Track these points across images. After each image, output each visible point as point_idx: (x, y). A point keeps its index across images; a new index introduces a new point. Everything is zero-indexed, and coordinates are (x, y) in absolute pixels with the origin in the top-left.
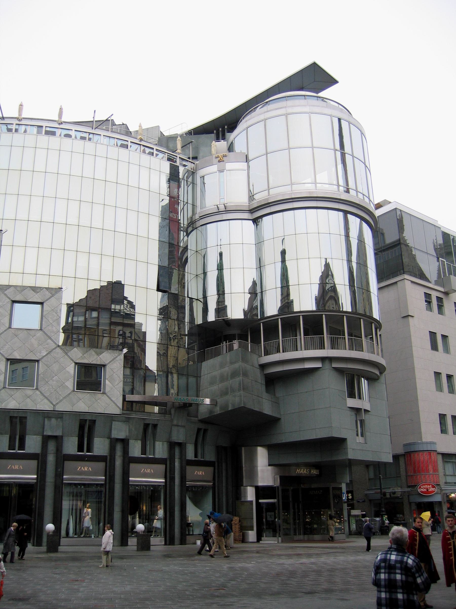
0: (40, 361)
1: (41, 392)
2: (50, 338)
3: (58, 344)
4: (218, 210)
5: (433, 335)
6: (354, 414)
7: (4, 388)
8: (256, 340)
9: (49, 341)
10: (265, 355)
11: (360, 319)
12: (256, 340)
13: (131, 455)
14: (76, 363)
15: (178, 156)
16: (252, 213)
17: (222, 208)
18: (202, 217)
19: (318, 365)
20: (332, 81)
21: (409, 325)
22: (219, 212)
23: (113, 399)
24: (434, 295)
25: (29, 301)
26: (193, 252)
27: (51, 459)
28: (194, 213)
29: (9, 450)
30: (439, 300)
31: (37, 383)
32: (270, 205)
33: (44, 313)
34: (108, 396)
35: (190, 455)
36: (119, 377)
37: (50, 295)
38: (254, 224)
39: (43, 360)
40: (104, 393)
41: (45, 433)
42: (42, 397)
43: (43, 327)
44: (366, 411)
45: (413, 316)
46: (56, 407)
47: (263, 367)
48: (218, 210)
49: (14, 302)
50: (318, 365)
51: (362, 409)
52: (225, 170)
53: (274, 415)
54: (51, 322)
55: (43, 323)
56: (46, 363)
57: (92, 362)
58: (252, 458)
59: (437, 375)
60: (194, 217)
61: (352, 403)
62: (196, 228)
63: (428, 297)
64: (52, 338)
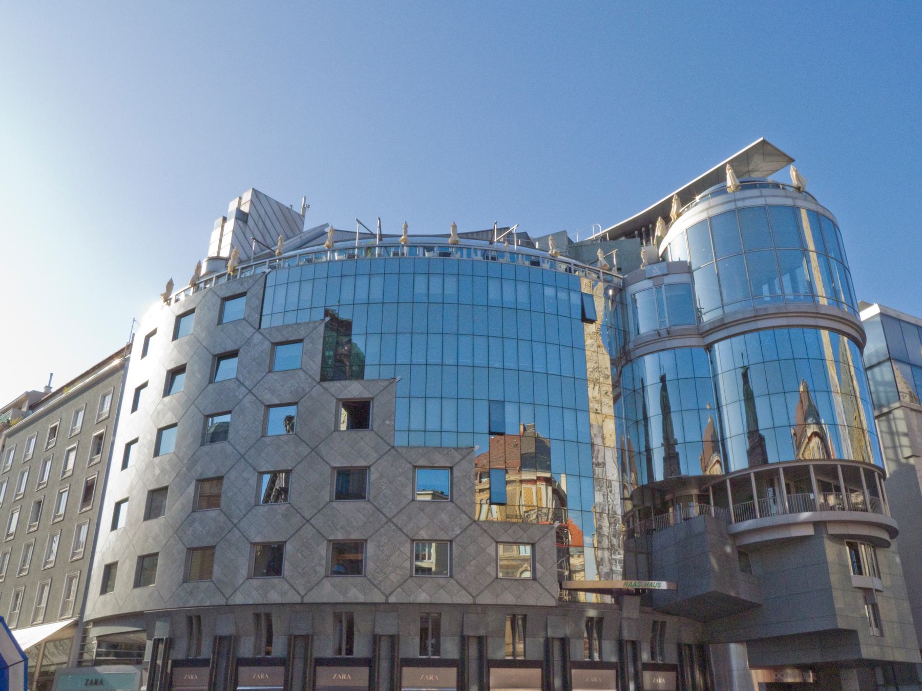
0: (454, 542)
1: (456, 581)
2: (463, 512)
4: (660, 336)
6: (862, 597)
7: (411, 576)
8: (721, 502)
9: (463, 516)
10: (737, 521)
11: (858, 468)
12: (721, 502)
15: (601, 271)
16: (703, 337)
18: (637, 347)
23: (547, 587)
25: (435, 465)
26: (629, 392)
28: (626, 342)
29: (421, 655)
31: (451, 569)
32: (727, 326)
33: (455, 480)
34: (540, 584)
35: (645, 657)
39: (457, 540)
41: (465, 633)
43: (455, 497)
44: (877, 590)
46: (477, 599)
47: (735, 536)
49: (415, 467)
50: (810, 531)
53: (754, 601)
54: (464, 491)
55: (454, 492)
56: (460, 544)
58: (726, 659)
60: (627, 347)
62: (631, 360)
64: (467, 512)
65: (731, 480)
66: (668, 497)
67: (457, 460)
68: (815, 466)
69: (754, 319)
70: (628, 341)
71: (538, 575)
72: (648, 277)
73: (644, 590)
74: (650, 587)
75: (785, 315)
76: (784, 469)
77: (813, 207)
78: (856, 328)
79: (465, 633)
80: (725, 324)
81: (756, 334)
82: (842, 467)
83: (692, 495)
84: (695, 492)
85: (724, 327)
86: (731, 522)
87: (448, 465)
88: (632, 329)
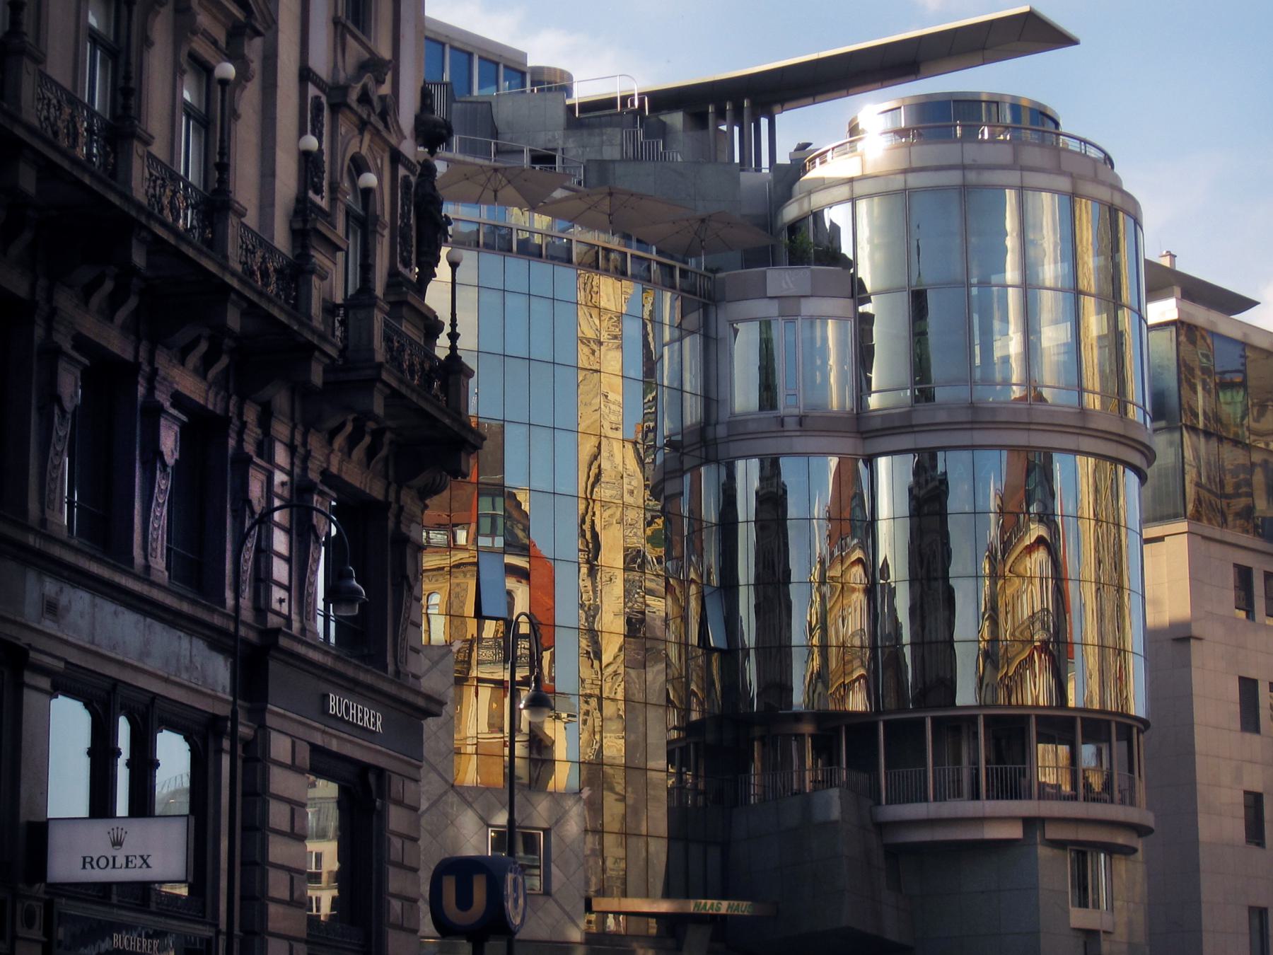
3: (451, 781)
8: (863, 759)
11: (1109, 722)
12: (863, 759)
16: (866, 438)
17: (791, 424)
20: (1059, 39)
21: (1187, 665)
22: (784, 431)
23: (568, 908)
32: (916, 429)
34: (556, 902)
38: (867, 467)
45: (1200, 639)
47: (882, 827)
48: (783, 426)
50: (1015, 832)
52: (799, 318)
56: (429, 828)
57: (522, 821)
60: (710, 429)
62: (718, 462)
63: (1244, 576)
65: (886, 723)
66: (757, 731)
68: (1037, 717)
69: (969, 426)
70: (713, 421)
71: (555, 886)
72: (768, 295)
73: (724, 917)
74: (736, 913)
75: (1027, 427)
76: (985, 716)
77: (1104, 194)
78: (1142, 448)
80: (912, 426)
81: (966, 455)
82: (1083, 719)
83: (803, 735)
84: (807, 728)
85: (910, 430)
86: (879, 803)
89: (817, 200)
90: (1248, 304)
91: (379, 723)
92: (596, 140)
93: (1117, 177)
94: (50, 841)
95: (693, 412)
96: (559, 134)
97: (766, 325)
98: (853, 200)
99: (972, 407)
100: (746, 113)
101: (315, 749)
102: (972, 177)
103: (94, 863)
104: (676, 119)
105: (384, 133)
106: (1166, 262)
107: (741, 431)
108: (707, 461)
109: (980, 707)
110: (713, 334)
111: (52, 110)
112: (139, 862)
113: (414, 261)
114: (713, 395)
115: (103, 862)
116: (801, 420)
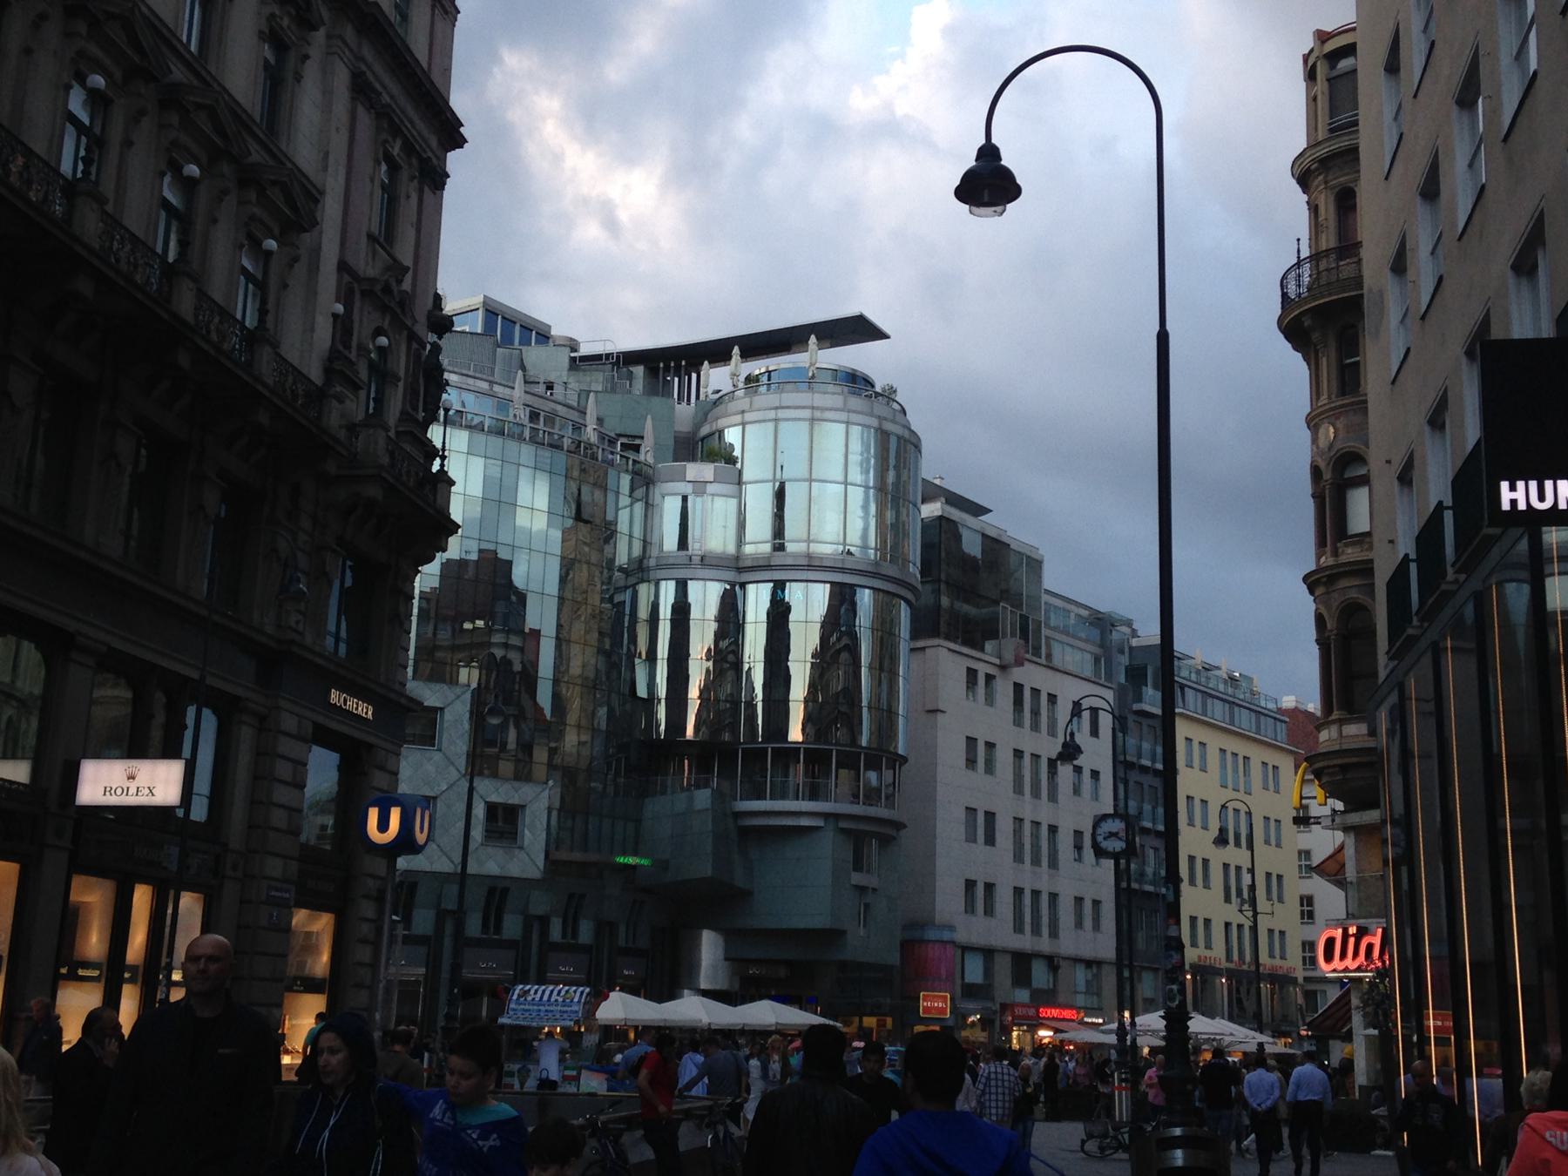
1: (438, 846)
2: (452, 764)
5: (971, 741)
8: (728, 772)
9: (451, 768)
13: (551, 940)
14: (486, 802)
17: (696, 560)
18: (659, 567)
19: (819, 823)
24: (982, 669)
27: (448, 943)
30: (989, 678)
36: (541, 823)
37: (453, 697)
39: (443, 797)
40: (521, 848)
41: (443, 906)
42: (440, 853)
44: (874, 890)
50: (819, 823)
51: (867, 888)
59: (971, 811)
60: (645, 561)
61: (857, 878)
63: (972, 674)
67: (450, 699)
70: (647, 556)
79: (443, 906)
87: (438, 704)
88: (655, 539)
89: (721, 423)
90: (986, 511)
91: (370, 713)
92: (588, 379)
93: (908, 421)
94: (80, 776)
95: (637, 551)
96: (565, 373)
97: (685, 499)
98: (744, 424)
99: (809, 556)
100: (683, 372)
101: (316, 725)
102: (818, 414)
103: (113, 792)
104: (639, 371)
105: (401, 316)
106: (937, 482)
107: (666, 565)
108: (642, 581)
109: (802, 743)
110: (650, 502)
111: (115, 243)
112: (147, 791)
113: (421, 409)
114: (649, 540)
115: (119, 791)
116: (703, 558)
